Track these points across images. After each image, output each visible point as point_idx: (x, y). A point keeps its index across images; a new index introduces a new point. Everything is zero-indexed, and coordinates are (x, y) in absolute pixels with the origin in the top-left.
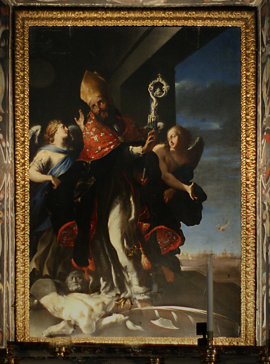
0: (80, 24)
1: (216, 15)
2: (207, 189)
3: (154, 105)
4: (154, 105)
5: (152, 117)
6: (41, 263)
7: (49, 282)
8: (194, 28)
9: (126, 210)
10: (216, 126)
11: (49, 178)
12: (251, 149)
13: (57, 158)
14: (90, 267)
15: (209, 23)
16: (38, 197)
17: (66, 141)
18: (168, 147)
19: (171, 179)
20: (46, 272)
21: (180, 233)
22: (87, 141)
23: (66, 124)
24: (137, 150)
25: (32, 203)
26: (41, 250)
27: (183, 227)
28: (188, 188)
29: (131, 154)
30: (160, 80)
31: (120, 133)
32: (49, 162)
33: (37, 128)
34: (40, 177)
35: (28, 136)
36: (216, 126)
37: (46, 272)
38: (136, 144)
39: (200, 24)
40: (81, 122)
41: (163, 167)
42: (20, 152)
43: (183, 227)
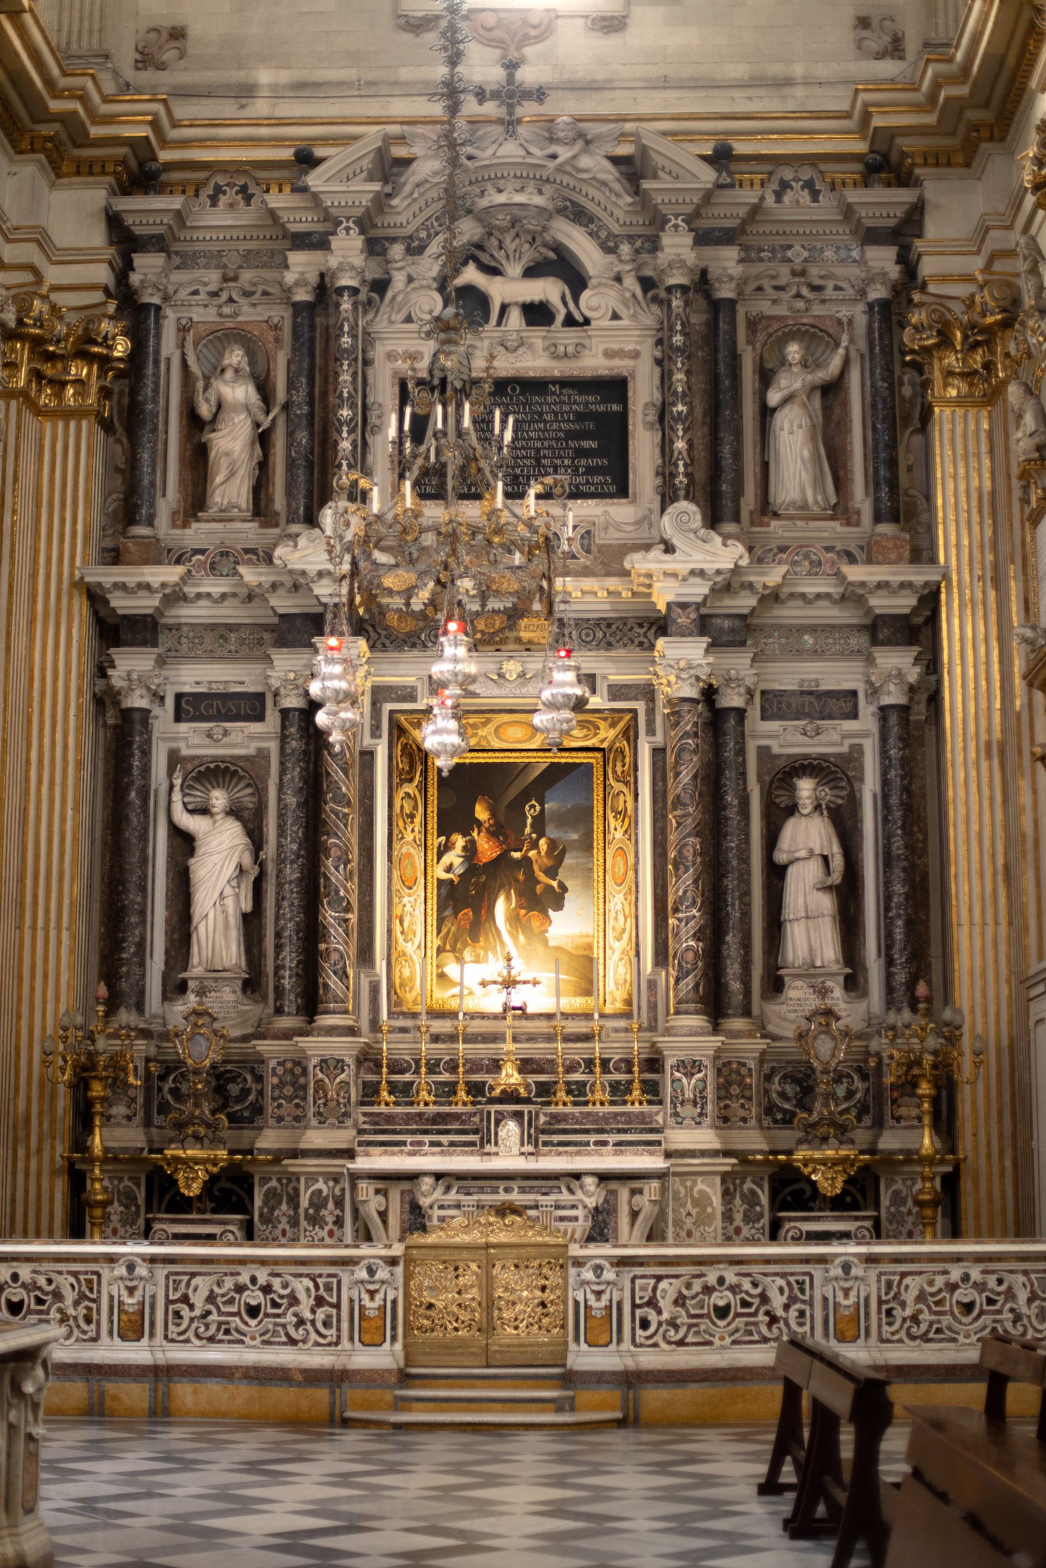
0: (475, 761)
1: (574, 754)
2: (568, 884)
3: (529, 821)
4: (529, 821)
5: (528, 830)
6: (444, 940)
7: (450, 955)
8: (559, 763)
9: (508, 898)
10: (575, 836)
11: (450, 876)
12: (601, 854)
13: (458, 862)
14: (481, 943)
15: (570, 761)
16: (444, 891)
17: (465, 848)
18: (539, 853)
19: (542, 877)
20: (448, 947)
21: (548, 917)
22: (480, 848)
23: (464, 836)
24: (516, 855)
25: (439, 895)
26: (444, 931)
27: (551, 912)
28: (555, 884)
29: (512, 858)
30: (533, 802)
31: (504, 842)
32: (451, 865)
33: (443, 839)
34: (445, 876)
35: (436, 845)
36: (575, 836)
37: (448, 947)
38: (516, 850)
39: (563, 761)
40: (475, 834)
41: (536, 867)
42: (429, 858)
43: (551, 912)
